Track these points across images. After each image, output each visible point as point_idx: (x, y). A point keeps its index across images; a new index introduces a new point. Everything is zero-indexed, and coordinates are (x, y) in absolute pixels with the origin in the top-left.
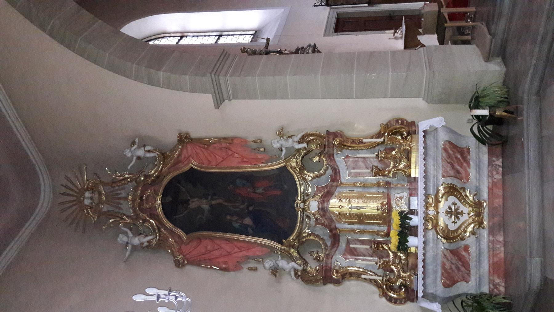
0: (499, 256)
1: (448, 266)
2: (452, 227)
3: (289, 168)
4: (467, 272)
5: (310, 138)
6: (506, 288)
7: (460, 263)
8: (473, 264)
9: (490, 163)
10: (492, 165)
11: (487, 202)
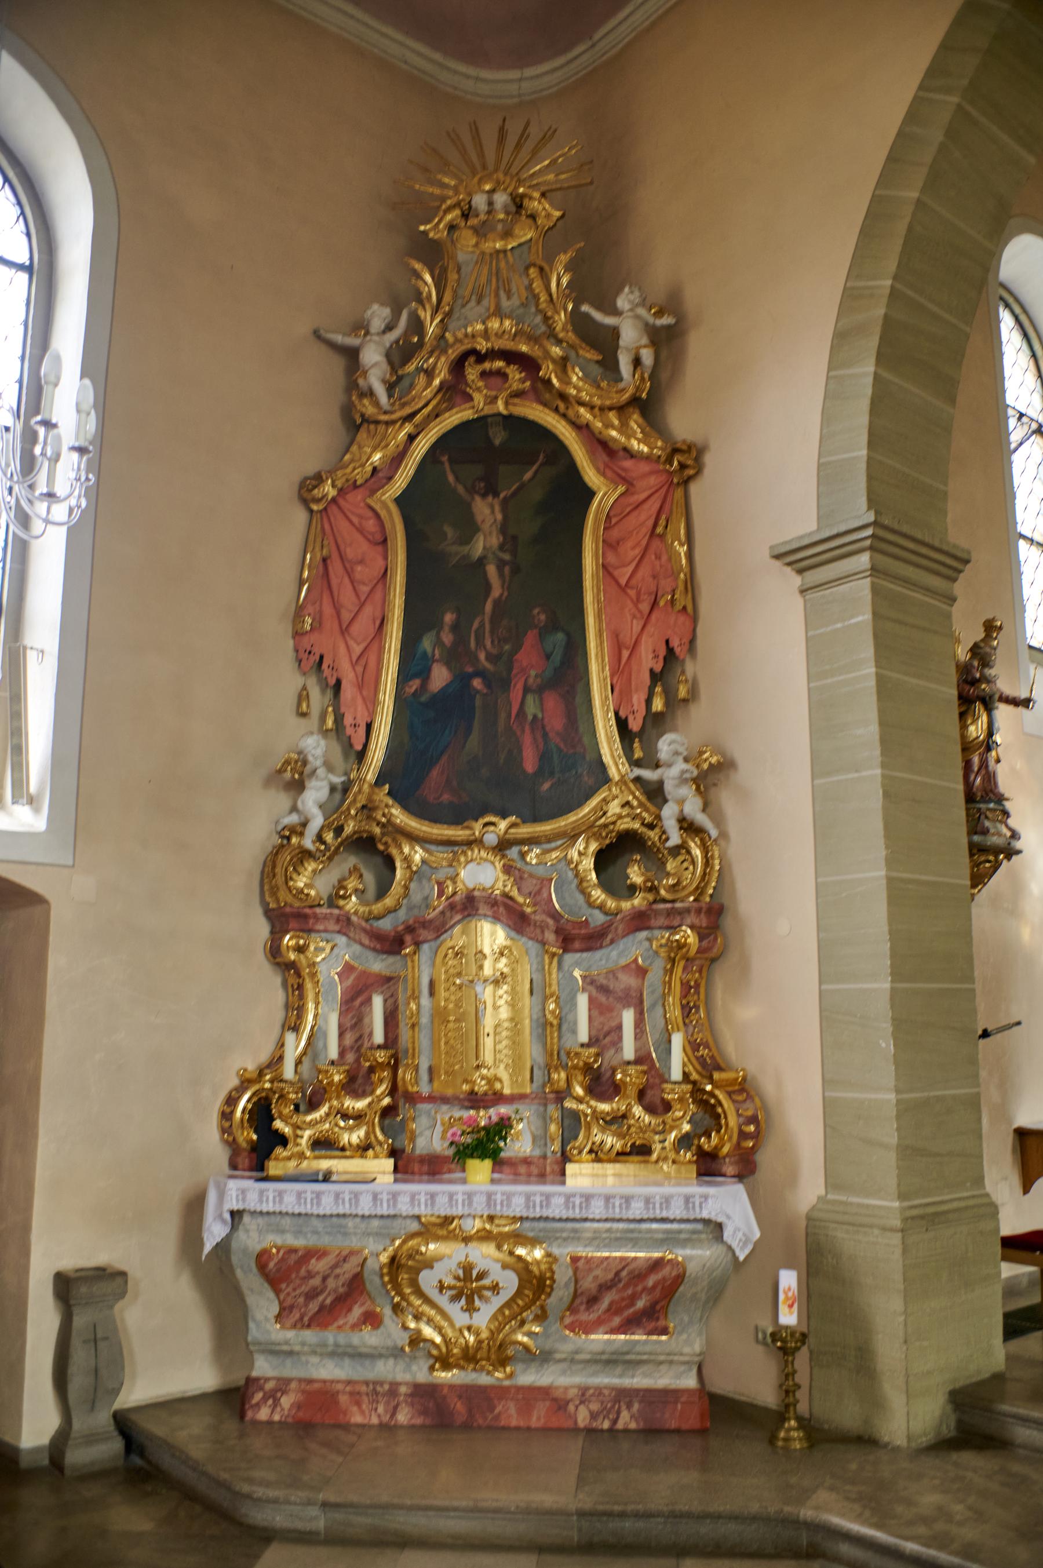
0: (355, 1409)
1: (319, 1266)
2: (428, 1280)
3: (602, 794)
4: (306, 1319)
5: (697, 852)
6: (270, 1423)
7: (328, 1301)
8: (330, 1336)
9: (624, 1396)
10: (617, 1400)
11: (507, 1383)
